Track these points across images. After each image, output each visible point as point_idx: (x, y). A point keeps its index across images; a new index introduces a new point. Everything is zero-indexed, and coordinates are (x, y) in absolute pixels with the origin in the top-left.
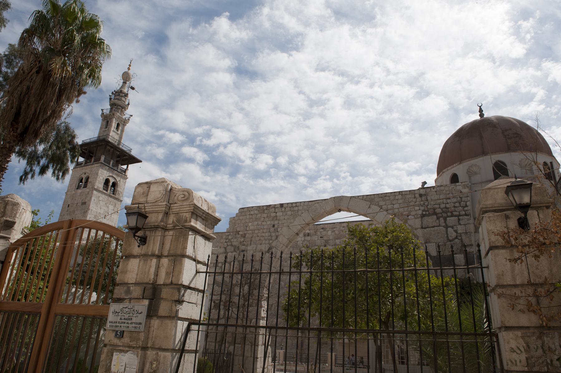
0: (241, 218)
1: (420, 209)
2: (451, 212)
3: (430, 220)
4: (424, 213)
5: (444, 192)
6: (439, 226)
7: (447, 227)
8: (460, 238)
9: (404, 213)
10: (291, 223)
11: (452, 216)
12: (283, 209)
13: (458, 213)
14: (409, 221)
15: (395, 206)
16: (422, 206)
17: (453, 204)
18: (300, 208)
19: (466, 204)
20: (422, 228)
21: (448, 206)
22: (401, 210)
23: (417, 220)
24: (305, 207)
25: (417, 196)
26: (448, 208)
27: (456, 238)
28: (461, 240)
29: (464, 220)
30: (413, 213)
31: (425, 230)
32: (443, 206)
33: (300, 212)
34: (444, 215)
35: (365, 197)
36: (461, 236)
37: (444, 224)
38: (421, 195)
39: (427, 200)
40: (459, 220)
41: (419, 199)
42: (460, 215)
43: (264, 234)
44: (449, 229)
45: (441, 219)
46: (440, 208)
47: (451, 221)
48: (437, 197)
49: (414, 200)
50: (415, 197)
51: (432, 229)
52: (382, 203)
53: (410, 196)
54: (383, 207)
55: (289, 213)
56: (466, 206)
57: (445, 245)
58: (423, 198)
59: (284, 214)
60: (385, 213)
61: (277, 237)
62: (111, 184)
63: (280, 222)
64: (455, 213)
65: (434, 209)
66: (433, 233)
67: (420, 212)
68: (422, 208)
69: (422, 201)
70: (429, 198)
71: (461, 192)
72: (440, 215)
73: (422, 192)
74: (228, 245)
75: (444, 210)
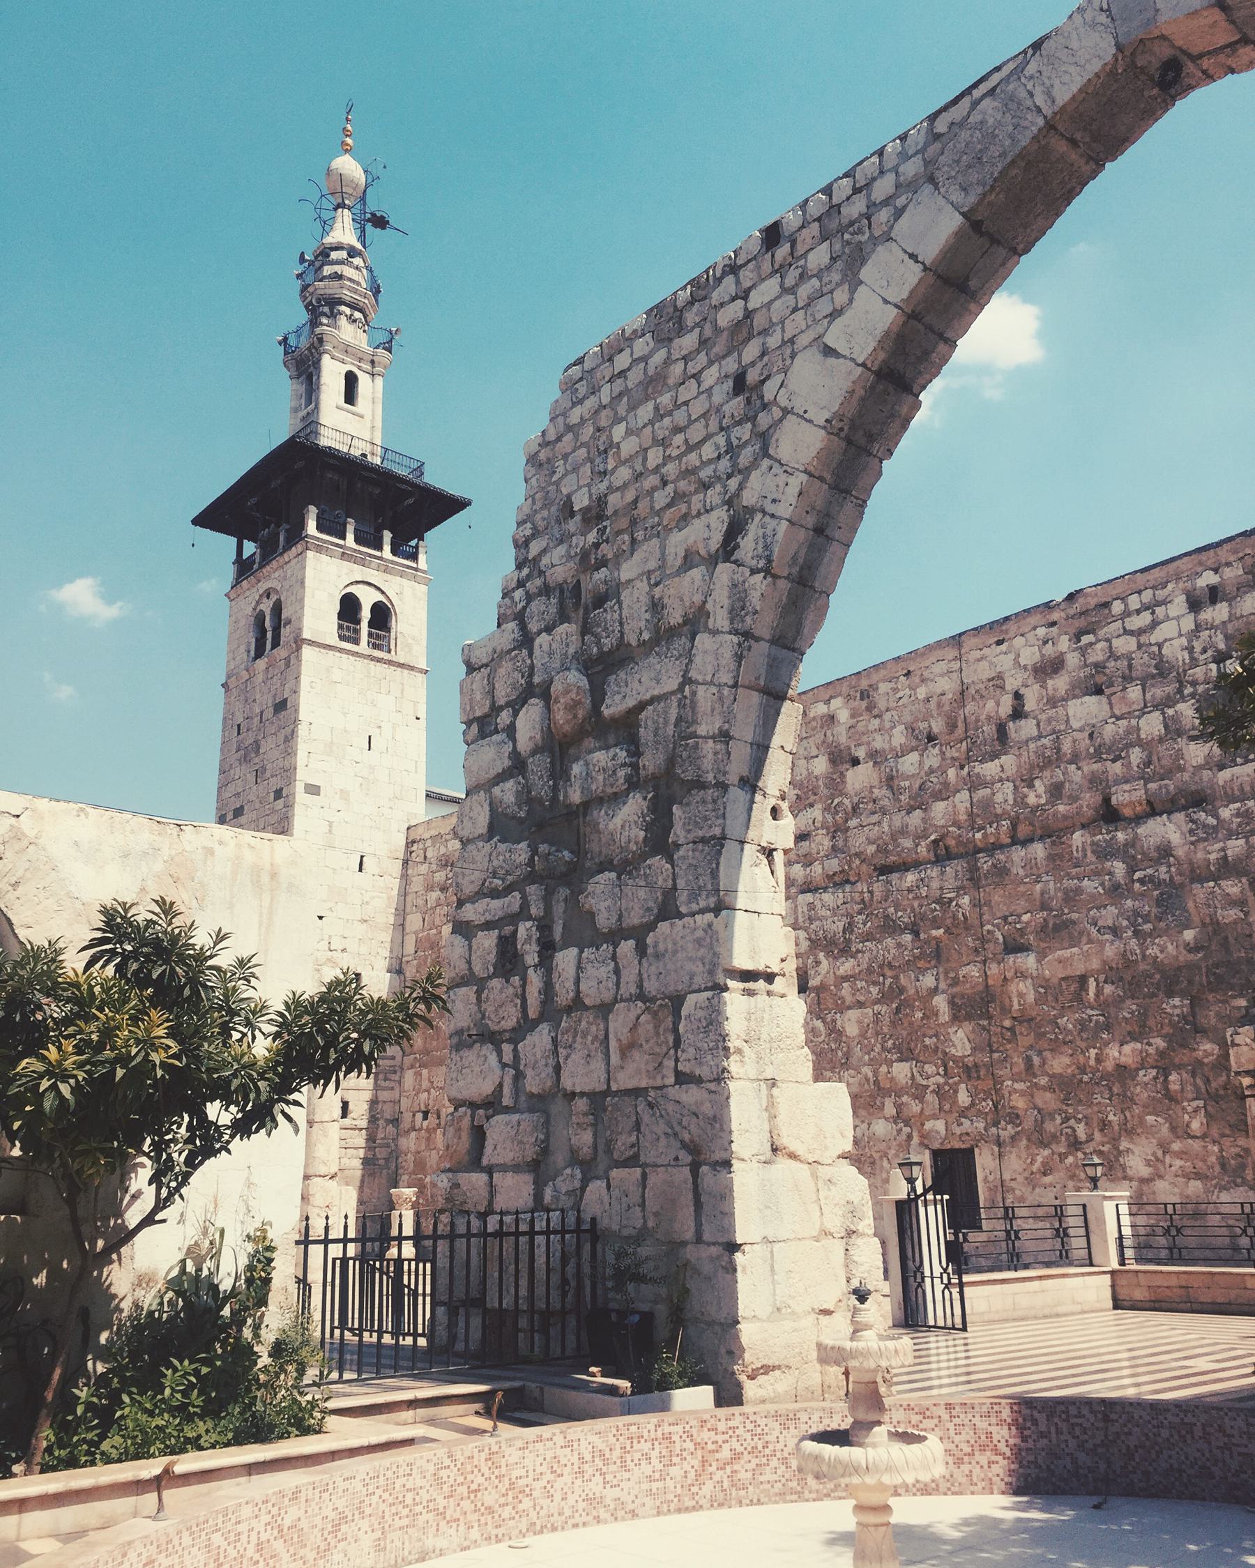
0: (575, 416)
43: (692, 459)
59: (792, 277)
61: (764, 439)
62: (366, 614)
63: (773, 341)
74: (529, 598)
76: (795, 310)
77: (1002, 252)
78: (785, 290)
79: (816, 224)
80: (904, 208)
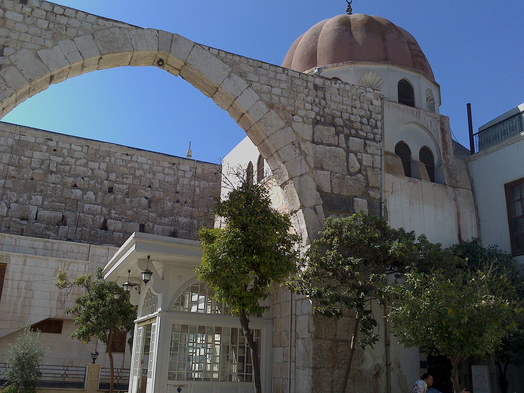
1: (312, 110)
2: (357, 131)
3: (327, 133)
4: (318, 118)
5: (350, 94)
6: (338, 146)
7: (348, 151)
8: (364, 173)
9: (288, 108)
10: (43, 47)
11: (357, 136)
12: (27, 9)
13: (365, 134)
14: (294, 125)
15: (274, 90)
16: (316, 105)
17: (359, 119)
18: (74, 23)
19: (376, 124)
20: (313, 142)
21: (353, 118)
22: (284, 100)
23: (306, 126)
24: (88, 27)
25: (311, 86)
26: (352, 122)
27: (360, 172)
28: (366, 177)
29: (373, 148)
30: (302, 113)
31: (318, 147)
32: (346, 116)
33: (72, 32)
34: (347, 131)
35: (223, 54)
36: (366, 170)
37: (345, 145)
38: (316, 87)
39: (325, 99)
40: (365, 144)
41: (313, 92)
42: (366, 139)
44: (352, 155)
45: (342, 136)
46: (341, 117)
47: (355, 143)
48: (339, 99)
49: (306, 91)
50: (307, 87)
51: (327, 148)
52: (253, 77)
53: (299, 82)
54: (254, 84)
55: (44, 24)
56: (376, 127)
57: (344, 179)
58: (320, 93)
59: (29, 21)
60: (257, 97)
63: (14, 36)
64: (361, 133)
65: (333, 118)
66: (328, 155)
67: (313, 115)
68: (317, 109)
69: (317, 96)
70: (328, 96)
71: (372, 104)
72: (340, 129)
73: (319, 82)
75: (348, 123)
76: (26, 32)
77: (96, 66)
78: (24, 22)
79: (45, 13)
80: (81, 35)
